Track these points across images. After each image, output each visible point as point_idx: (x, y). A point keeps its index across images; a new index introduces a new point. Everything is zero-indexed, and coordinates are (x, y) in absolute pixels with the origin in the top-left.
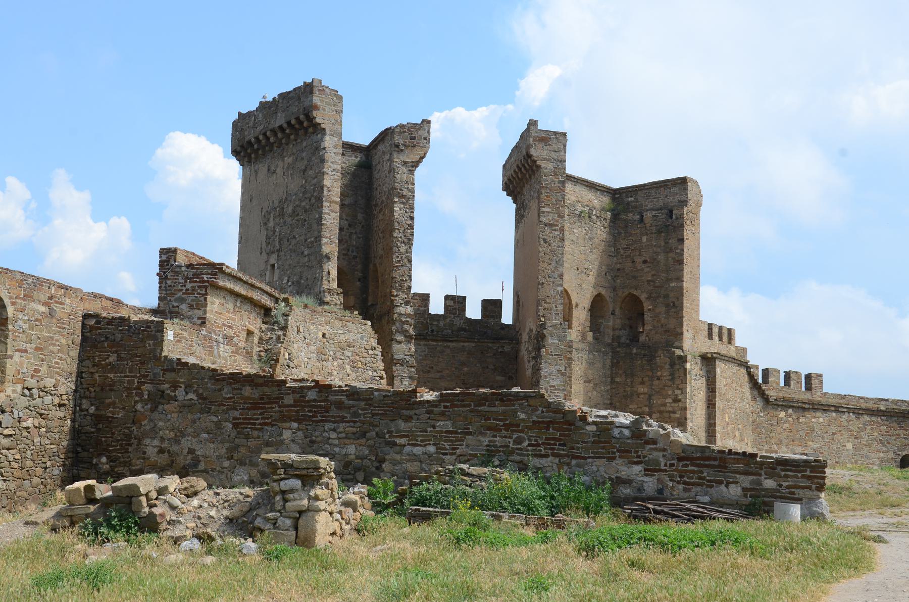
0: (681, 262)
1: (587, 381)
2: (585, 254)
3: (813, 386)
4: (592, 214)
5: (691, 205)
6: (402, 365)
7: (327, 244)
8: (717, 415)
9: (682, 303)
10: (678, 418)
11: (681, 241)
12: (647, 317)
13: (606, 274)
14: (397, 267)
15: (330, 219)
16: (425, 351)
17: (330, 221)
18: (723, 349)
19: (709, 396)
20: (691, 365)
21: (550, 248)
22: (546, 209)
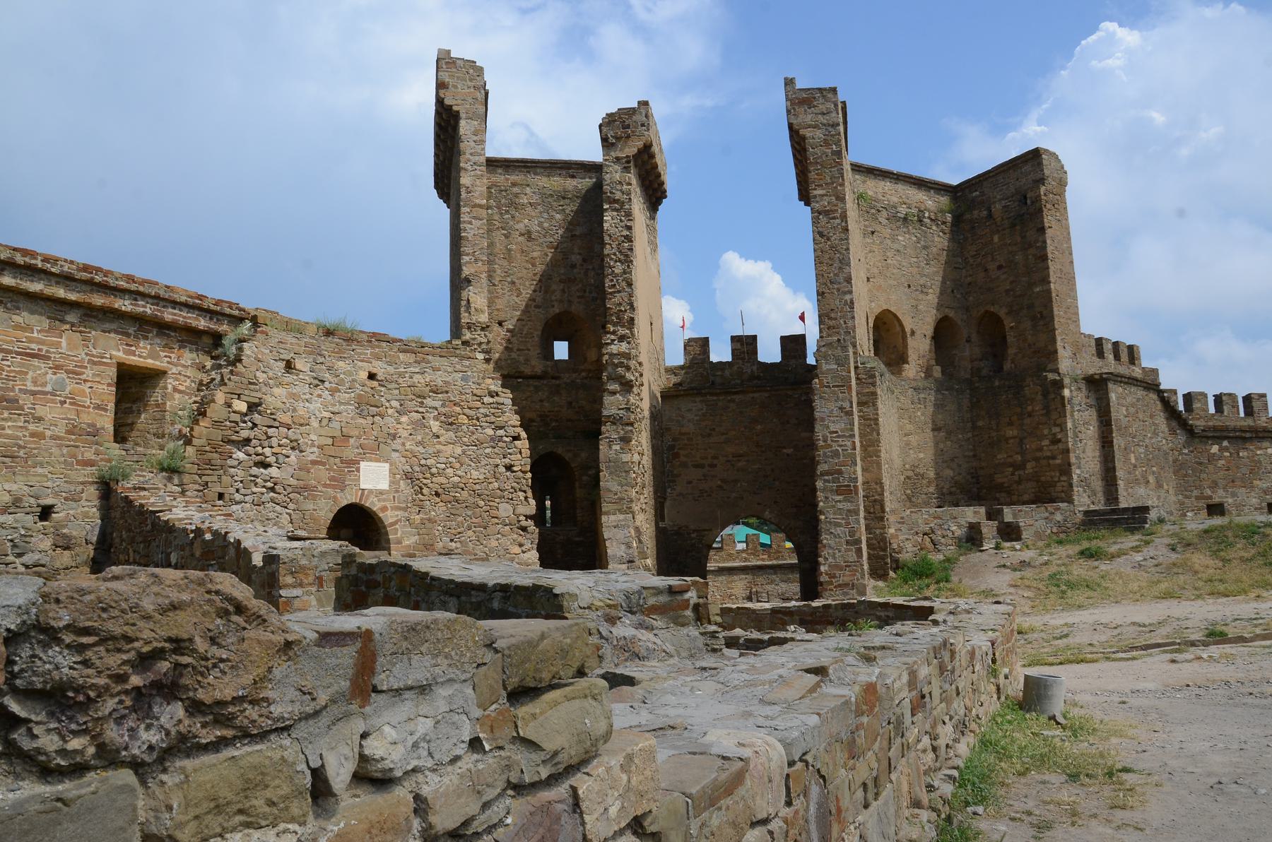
0: (1044, 258)
1: (936, 429)
2: (918, 267)
3: (1256, 409)
4: (924, 217)
5: (1051, 184)
6: (614, 423)
7: (470, 263)
8: (1117, 457)
9: (1052, 311)
10: (1059, 465)
11: (1042, 230)
12: (1011, 339)
13: (953, 291)
14: (611, 293)
15: (471, 229)
16: (702, 409)
17: (472, 232)
18: (1123, 369)
19: (1103, 432)
20: (1071, 391)
21: (829, 243)
22: (819, 192)
